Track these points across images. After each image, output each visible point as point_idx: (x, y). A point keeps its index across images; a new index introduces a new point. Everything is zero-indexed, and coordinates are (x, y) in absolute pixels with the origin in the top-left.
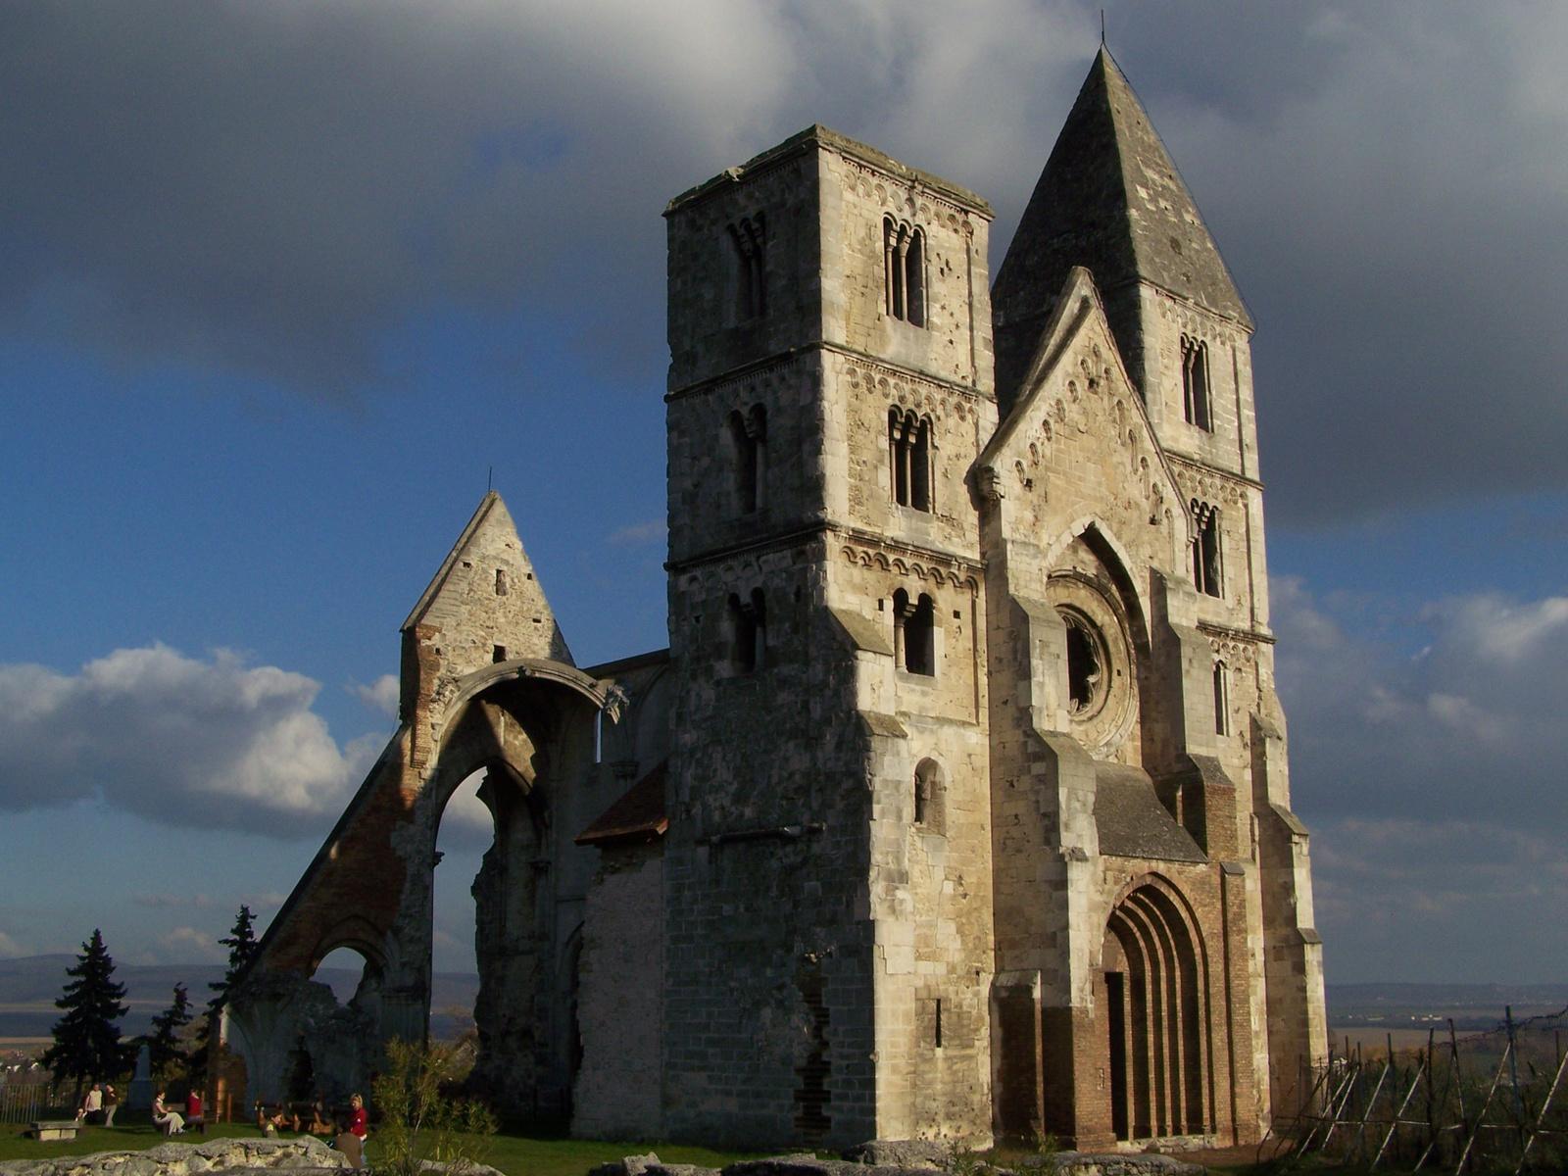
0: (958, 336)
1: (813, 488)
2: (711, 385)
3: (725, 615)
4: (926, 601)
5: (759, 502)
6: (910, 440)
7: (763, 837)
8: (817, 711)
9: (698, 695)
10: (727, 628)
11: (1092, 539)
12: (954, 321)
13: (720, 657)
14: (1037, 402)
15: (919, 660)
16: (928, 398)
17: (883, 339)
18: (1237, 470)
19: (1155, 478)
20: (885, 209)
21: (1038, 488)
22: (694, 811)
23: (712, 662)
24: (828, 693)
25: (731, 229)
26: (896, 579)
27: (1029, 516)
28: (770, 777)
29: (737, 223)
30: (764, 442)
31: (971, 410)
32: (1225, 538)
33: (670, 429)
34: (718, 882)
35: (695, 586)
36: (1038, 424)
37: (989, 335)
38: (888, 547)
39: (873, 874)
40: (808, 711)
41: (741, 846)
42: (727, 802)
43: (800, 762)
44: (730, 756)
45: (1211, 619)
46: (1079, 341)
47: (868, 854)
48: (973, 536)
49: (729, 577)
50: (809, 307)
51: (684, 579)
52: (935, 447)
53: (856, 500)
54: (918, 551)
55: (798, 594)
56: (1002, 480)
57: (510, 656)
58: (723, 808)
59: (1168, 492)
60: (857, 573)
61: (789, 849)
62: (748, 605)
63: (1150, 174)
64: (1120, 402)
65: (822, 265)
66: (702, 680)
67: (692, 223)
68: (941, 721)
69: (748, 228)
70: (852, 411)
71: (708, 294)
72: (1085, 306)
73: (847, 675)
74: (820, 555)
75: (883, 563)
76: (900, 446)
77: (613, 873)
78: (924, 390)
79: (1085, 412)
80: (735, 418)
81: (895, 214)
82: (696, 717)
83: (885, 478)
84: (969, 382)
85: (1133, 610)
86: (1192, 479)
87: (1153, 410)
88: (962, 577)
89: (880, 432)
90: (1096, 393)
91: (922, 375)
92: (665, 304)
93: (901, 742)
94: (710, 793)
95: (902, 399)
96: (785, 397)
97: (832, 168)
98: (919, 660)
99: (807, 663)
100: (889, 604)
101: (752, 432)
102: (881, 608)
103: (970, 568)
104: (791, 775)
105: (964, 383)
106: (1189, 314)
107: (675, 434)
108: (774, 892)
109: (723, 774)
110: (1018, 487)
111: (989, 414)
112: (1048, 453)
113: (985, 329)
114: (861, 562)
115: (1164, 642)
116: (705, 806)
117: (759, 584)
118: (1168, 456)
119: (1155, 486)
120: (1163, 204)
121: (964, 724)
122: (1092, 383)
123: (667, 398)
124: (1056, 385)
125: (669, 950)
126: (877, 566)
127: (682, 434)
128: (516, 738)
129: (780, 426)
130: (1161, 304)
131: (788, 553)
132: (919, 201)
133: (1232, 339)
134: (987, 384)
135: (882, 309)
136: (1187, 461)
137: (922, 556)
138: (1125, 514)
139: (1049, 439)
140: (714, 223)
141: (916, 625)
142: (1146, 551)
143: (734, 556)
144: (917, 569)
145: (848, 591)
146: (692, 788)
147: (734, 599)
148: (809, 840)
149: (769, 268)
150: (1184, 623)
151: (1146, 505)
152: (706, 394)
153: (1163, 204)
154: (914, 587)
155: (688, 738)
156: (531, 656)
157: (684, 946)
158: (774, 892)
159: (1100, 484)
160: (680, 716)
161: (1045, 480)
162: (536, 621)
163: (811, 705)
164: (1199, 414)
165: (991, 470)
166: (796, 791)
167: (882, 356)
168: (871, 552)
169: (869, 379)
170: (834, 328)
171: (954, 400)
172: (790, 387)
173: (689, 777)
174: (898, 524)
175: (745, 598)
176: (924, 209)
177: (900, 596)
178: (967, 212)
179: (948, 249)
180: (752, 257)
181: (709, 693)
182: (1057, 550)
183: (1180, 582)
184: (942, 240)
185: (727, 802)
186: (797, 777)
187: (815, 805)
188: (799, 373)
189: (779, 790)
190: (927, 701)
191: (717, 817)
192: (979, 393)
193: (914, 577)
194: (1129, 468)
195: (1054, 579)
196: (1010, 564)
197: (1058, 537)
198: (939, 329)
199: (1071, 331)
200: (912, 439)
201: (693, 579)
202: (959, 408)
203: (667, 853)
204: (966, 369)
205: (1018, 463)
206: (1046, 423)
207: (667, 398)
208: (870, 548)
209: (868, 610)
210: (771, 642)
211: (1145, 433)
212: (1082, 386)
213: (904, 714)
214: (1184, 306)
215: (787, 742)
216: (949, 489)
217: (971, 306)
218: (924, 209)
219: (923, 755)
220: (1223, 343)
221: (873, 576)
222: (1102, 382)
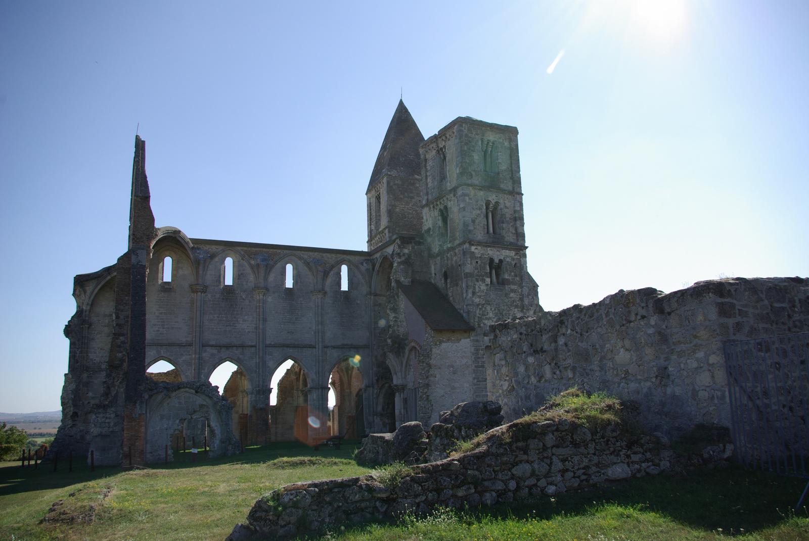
23: (484, 278)
24: (530, 297)
44: (493, 309)
66: (481, 283)
69: (488, 143)
94: (486, 320)
109: (491, 315)
117: (502, 258)
125: (474, 370)
143: (494, 247)
157: (481, 369)
163: (525, 299)
175: (497, 261)
181: (483, 287)
203: (472, 338)
215: (515, 308)
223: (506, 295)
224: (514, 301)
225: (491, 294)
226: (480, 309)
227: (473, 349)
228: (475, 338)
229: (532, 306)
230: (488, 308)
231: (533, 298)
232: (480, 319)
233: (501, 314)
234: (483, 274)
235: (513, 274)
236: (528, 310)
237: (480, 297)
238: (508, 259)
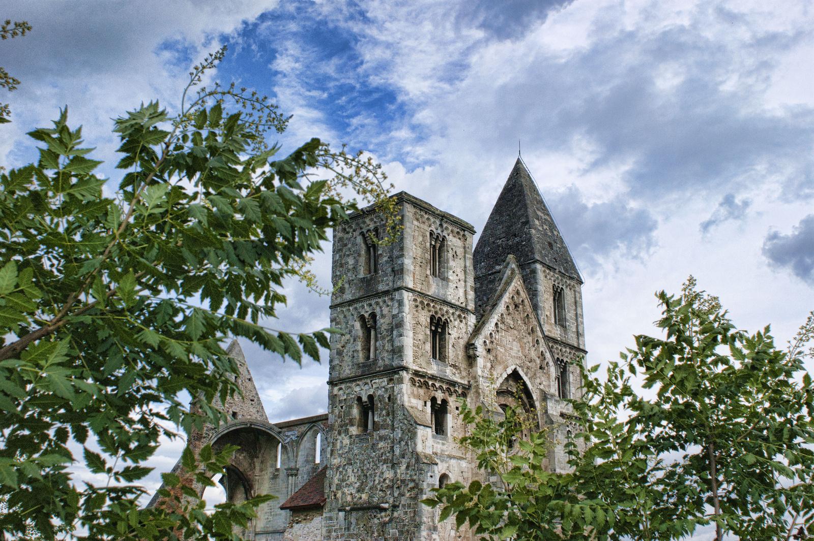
0: (459, 287)
1: (398, 351)
2: (350, 303)
3: (355, 406)
4: (445, 402)
5: (372, 355)
6: (438, 329)
7: (372, 508)
8: (397, 452)
9: (342, 442)
10: (355, 412)
11: (515, 376)
12: (458, 278)
13: (352, 425)
14: (493, 315)
15: (440, 428)
16: (447, 312)
17: (429, 286)
18: (576, 345)
19: (541, 349)
20: (430, 229)
21: (494, 353)
22: (338, 495)
24: (403, 443)
25: (362, 234)
26: (433, 393)
27: (489, 365)
28: (374, 481)
29: (364, 231)
30: (375, 330)
31: (465, 318)
32: (571, 375)
33: (332, 321)
34: (348, 529)
35: (341, 392)
36: (493, 325)
37: (473, 284)
38: (429, 378)
39: (423, 527)
40: (393, 451)
41: (360, 513)
42: (354, 491)
43: (389, 475)
44: (355, 471)
45: (564, 411)
46: (511, 289)
47: (421, 517)
48: (464, 374)
49: (357, 389)
50: (399, 272)
51: (336, 389)
52: (449, 334)
53: (416, 357)
54: (442, 380)
55: (389, 398)
56: (478, 349)
57: (240, 417)
58: (352, 494)
59: (548, 355)
60: (415, 389)
61: (383, 514)
62: (366, 402)
63: (539, 213)
64: (528, 315)
65: (404, 253)
66: (343, 435)
67: (344, 230)
68: (451, 457)
70: (414, 318)
71: (351, 261)
72: (513, 270)
73: (413, 436)
74: (401, 381)
75: (426, 384)
76: (434, 333)
77: (297, 523)
78: (445, 308)
79: (513, 319)
80: (362, 318)
81: (435, 230)
82: (340, 452)
83: (428, 346)
84: (463, 305)
85: (532, 405)
86: (557, 348)
87: (542, 318)
88: (460, 392)
89: (426, 327)
90: (517, 311)
91: (445, 302)
92: (331, 265)
93: (435, 467)
95: (436, 313)
96: (385, 310)
97: (409, 210)
98: (440, 428)
99: (393, 429)
100: (429, 404)
101: (369, 325)
102: (425, 406)
103: (464, 388)
104: (385, 480)
105: (462, 305)
106: (556, 276)
107: (334, 323)
108: (376, 534)
109: (352, 479)
110: (484, 353)
111: (472, 320)
112: (497, 337)
113: (471, 282)
114: (417, 384)
115: (546, 422)
116: (343, 493)
117: (371, 393)
118: (547, 338)
119: (542, 352)
120: (545, 227)
121: (461, 458)
122: (516, 306)
123: (331, 307)
124: (501, 308)
126: (424, 386)
127: (337, 324)
128: (240, 455)
129: (383, 323)
130: (544, 271)
131: (385, 379)
132: (445, 225)
133: (573, 286)
134: (471, 306)
135: (428, 272)
136: (555, 341)
137: (443, 382)
138: (529, 364)
139: (498, 331)
140: (354, 231)
141: (439, 411)
142: (538, 381)
143: (360, 380)
144: (441, 388)
145: (411, 398)
146: (337, 485)
147: (359, 399)
148: (393, 511)
149: (380, 252)
150: (555, 413)
151: (538, 361)
152: (349, 306)
153: (545, 227)
154: (440, 396)
155: (336, 461)
156: (249, 417)
158: (376, 534)
159: (519, 351)
160: (332, 451)
161: (496, 349)
162: (252, 400)
164: (561, 321)
165: (473, 344)
166: (388, 487)
167: (430, 294)
168: (422, 380)
169: (422, 303)
170: (409, 282)
171: (457, 313)
172: (388, 306)
173: (336, 481)
174: (433, 369)
175: (365, 399)
176: (447, 228)
177: (434, 400)
178: (464, 231)
179: (456, 246)
180: (372, 248)
181: (347, 441)
182: (501, 380)
183: (552, 396)
184: (453, 242)
185: (354, 491)
186: (387, 481)
187: (396, 494)
188: (392, 299)
189: (379, 487)
190: (444, 448)
191: (349, 498)
192: (468, 310)
193: (440, 391)
194: (531, 344)
195: (500, 393)
196: (481, 387)
197: (501, 374)
198: (452, 281)
199: (508, 284)
200: (440, 330)
201: (341, 389)
202: (459, 316)
203: (324, 515)
204: (462, 300)
205: (485, 342)
206: (496, 324)
207: (331, 307)
208: (421, 379)
209: (419, 404)
210: (376, 419)
211: (538, 329)
212: (511, 307)
213: (436, 454)
214: (554, 272)
216: (454, 352)
217: (465, 272)
218: (447, 228)
219: (443, 472)
220: (570, 289)
221: (422, 391)
222: (521, 306)
223: (374, 447)
224: (382, 454)
225: (355, 448)
226: (341, 473)
227: (324, 530)
228: (328, 515)
229: (404, 458)
230: (350, 471)
231: (407, 444)
232: (339, 487)
233: (366, 475)
234: (347, 421)
235: (384, 412)
236: (398, 464)
237: (340, 456)
238: (380, 392)
